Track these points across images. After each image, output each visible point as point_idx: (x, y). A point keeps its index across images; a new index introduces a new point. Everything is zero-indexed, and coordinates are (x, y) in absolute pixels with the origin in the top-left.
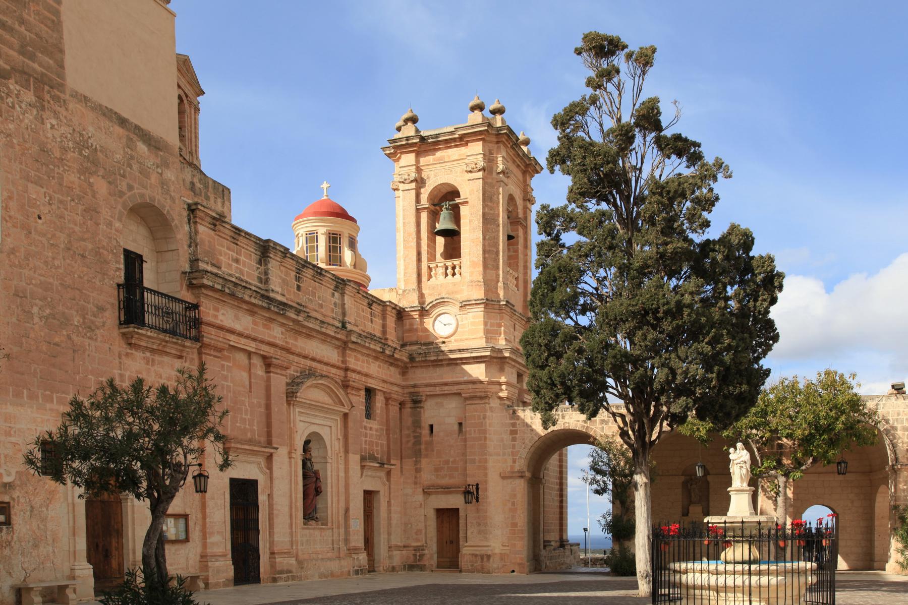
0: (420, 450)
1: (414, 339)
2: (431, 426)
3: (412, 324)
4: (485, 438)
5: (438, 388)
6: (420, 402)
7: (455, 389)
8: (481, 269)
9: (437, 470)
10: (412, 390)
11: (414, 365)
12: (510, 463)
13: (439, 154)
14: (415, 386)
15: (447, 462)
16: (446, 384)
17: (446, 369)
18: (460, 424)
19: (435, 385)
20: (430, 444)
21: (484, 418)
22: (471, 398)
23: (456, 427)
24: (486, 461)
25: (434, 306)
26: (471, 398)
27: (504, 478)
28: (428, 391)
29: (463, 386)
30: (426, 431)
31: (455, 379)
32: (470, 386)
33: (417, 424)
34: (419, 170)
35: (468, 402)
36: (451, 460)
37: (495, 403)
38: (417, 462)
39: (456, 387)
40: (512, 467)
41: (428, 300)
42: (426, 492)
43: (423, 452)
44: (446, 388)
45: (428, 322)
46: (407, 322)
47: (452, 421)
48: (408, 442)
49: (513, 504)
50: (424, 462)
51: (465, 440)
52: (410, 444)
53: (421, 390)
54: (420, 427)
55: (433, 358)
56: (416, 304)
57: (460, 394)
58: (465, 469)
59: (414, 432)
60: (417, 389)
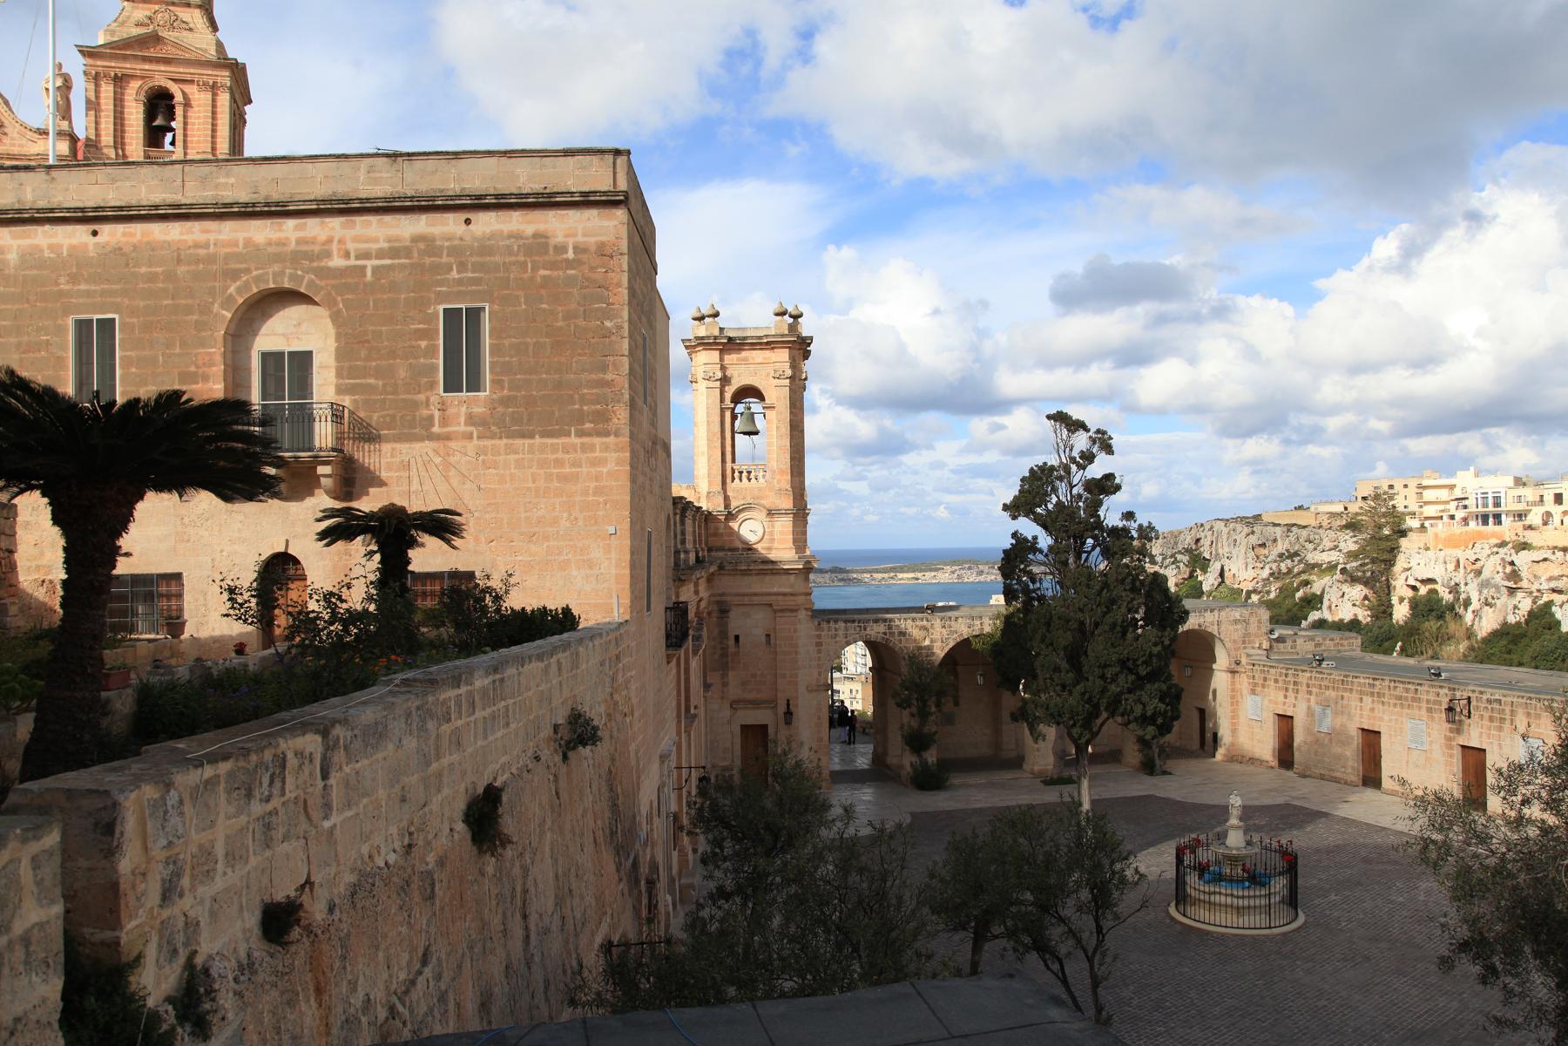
0: (727, 663)
1: (719, 544)
2: (737, 638)
3: (717, 529)
4: (796, 653)
5: (746, 598)
6: (728, 611)
7: (766, 599)
8: (789, 477)
9: (744, 684)
10: (719, 598)
11: (722, 572)
12: (816, 675)
13: (744, 354)
14: (722, 595)
15: (754, 676)
16: (755, 594)
17: (755, 578)
18: (768, 636)
19: (744, 595)
20: (737, 654)
21: (795, 631)
22: (782, 611)
23: (763, 639)
24: (796, 675)
25: (740, 511)
26: (782, 611)
27: (810, 691)
28: (736, 600)
29: (773, 598)
30: (732, 642)
31: (764, 590)
32: (780, 598)
33: (723, 634)
34: (723, 368)
35: (778, 614)
36: (759, 673)
37: (802, 615)
38: (724, 676)
39: (766, 598)
40: (818, 680)
41: (734, 504)
42: (735, 705)
43: (730, 664)
44: (755, 598)
45: (734, 525)
46: (712, 526)
47: (759, 633)
48: (714, 653)
49: (819, 718)
50: (731, 673)
51: (776, 653)
52: (717, 657)
53: (729, 599)
54: (727, 638)
55: (743, 568)
56: (722, 508)
57: (771, 605)
58: (775, 683)
59: (721, 643)
60: (724, 598)
